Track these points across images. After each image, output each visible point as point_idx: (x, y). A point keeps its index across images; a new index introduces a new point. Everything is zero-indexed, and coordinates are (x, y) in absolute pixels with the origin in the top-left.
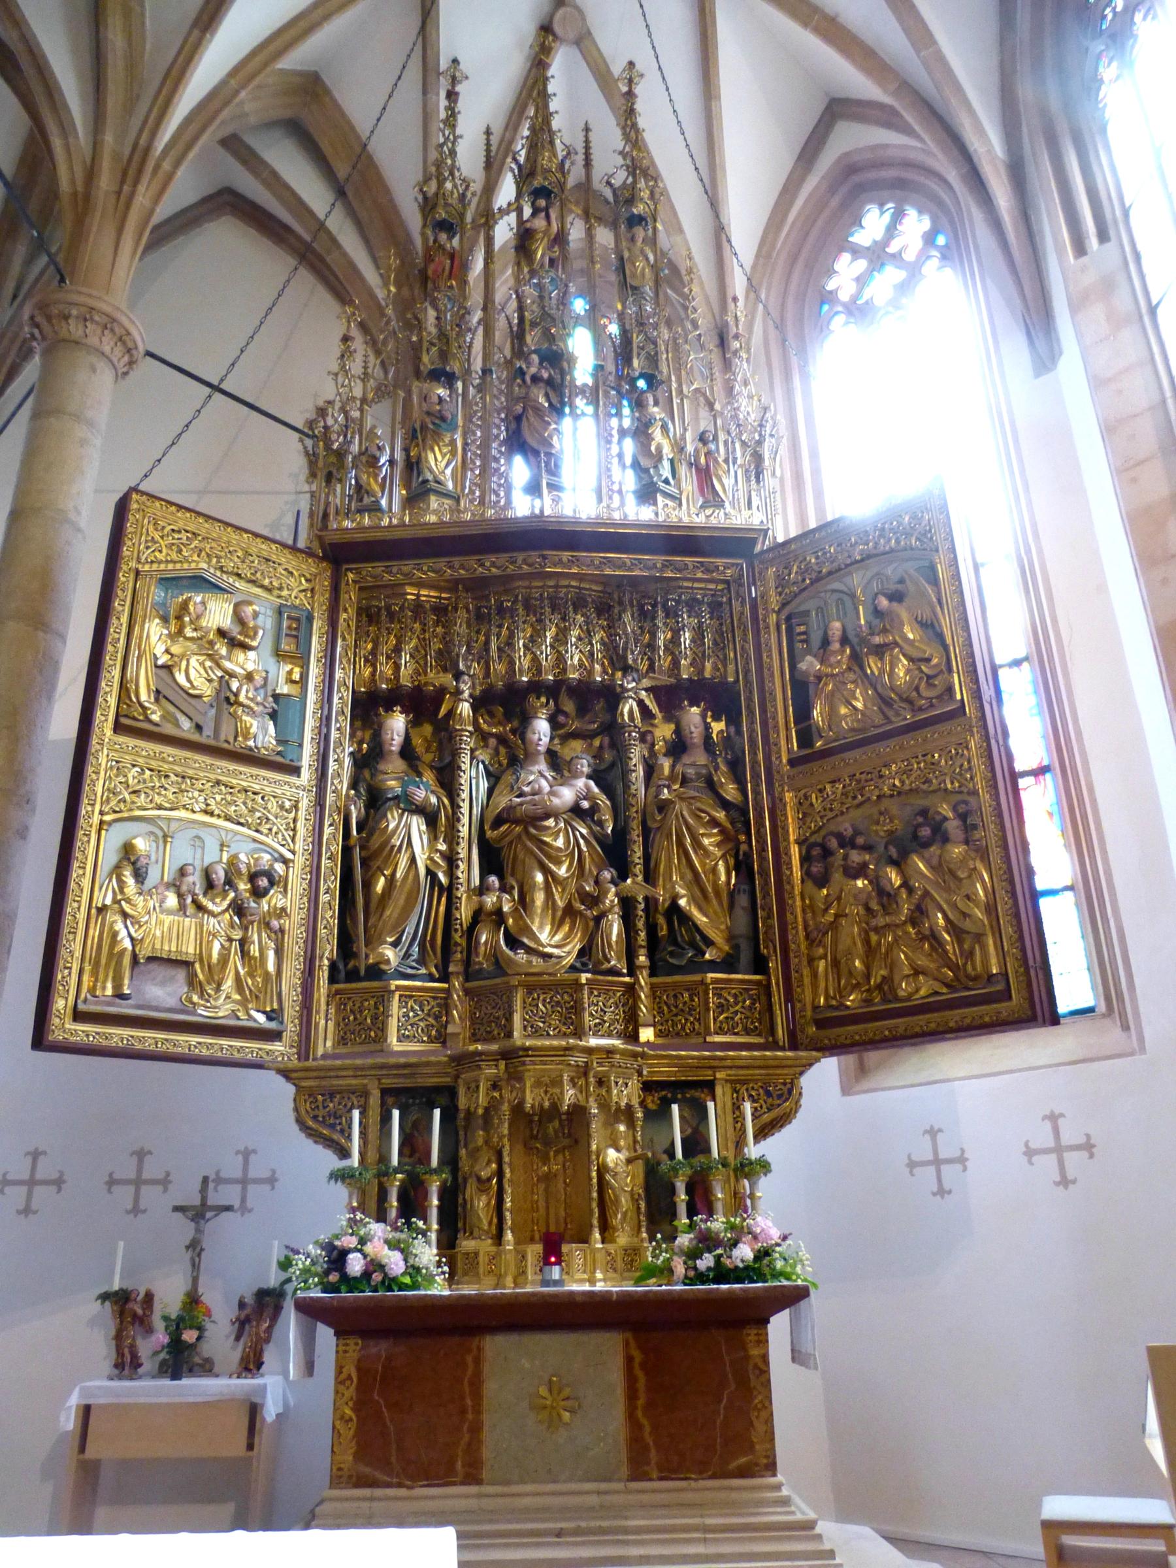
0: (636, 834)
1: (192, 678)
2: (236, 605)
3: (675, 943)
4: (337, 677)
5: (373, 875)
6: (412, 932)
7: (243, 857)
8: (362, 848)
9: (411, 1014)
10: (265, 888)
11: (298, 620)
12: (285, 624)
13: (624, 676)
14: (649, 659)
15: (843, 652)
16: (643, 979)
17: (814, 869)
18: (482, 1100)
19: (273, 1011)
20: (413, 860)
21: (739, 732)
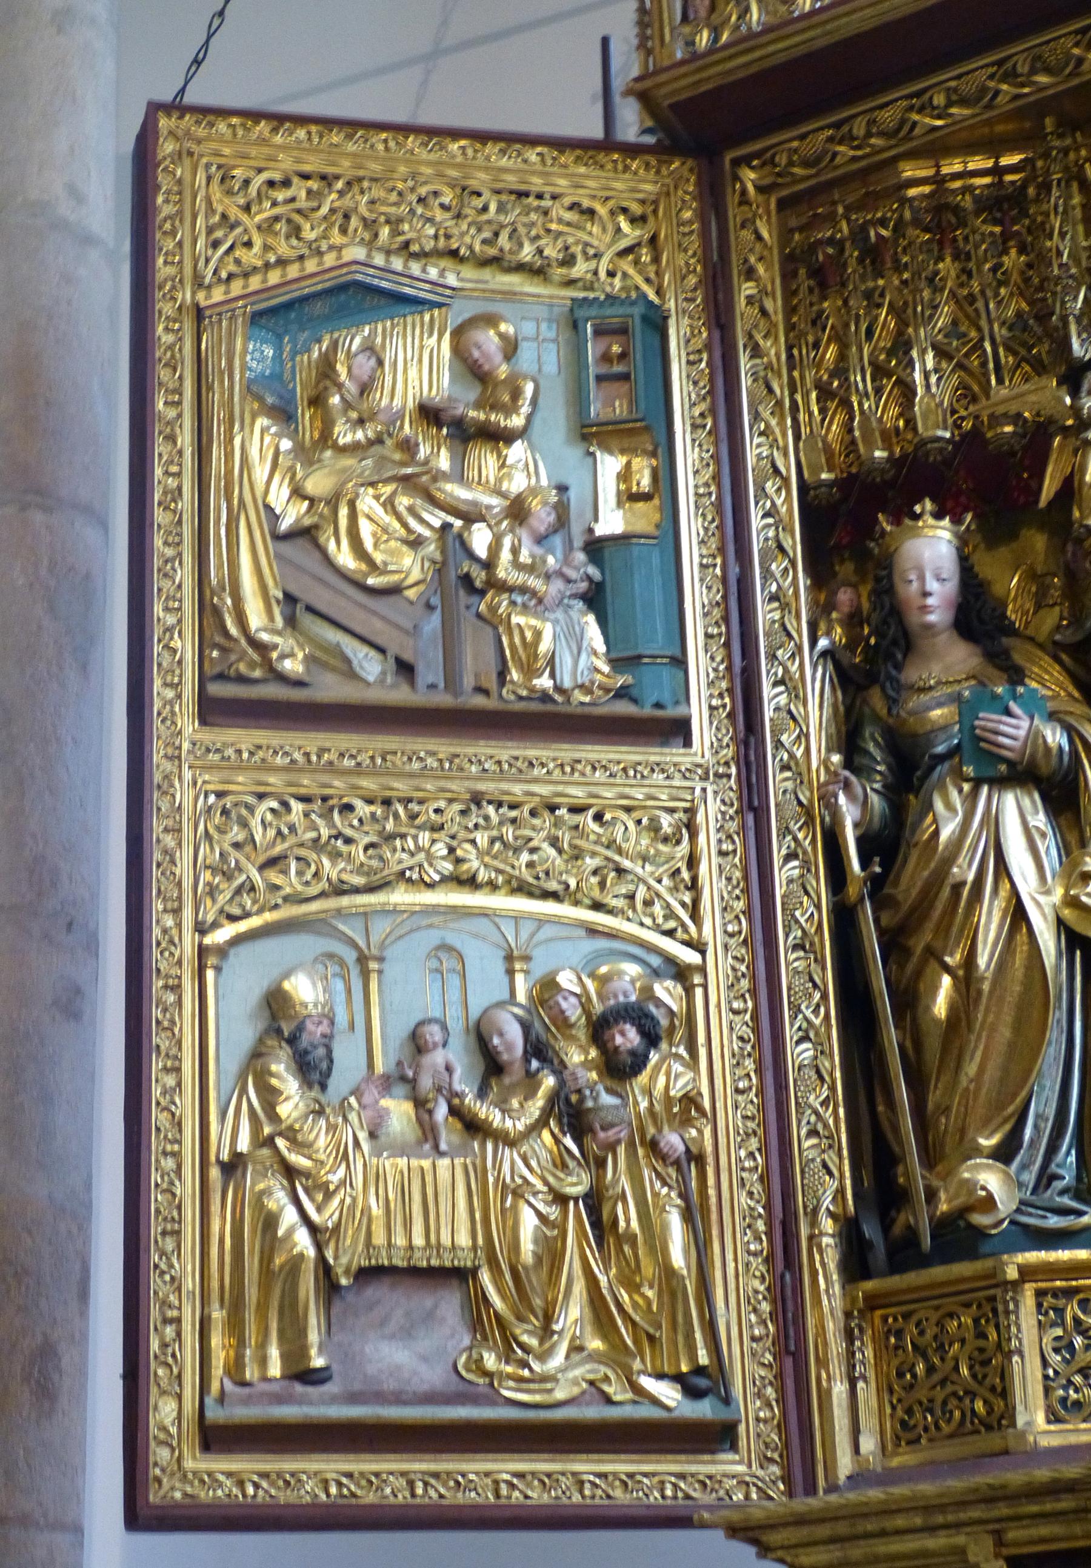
1: (368, 544)
2: (458, 333)
4: (750, 460)
6: (1051, 1112)
7: (566, 980)
10: (633, 1053)
11: (623, 331)
12: (592, 351)
19: (699, 1371)
20: (1018, 914)
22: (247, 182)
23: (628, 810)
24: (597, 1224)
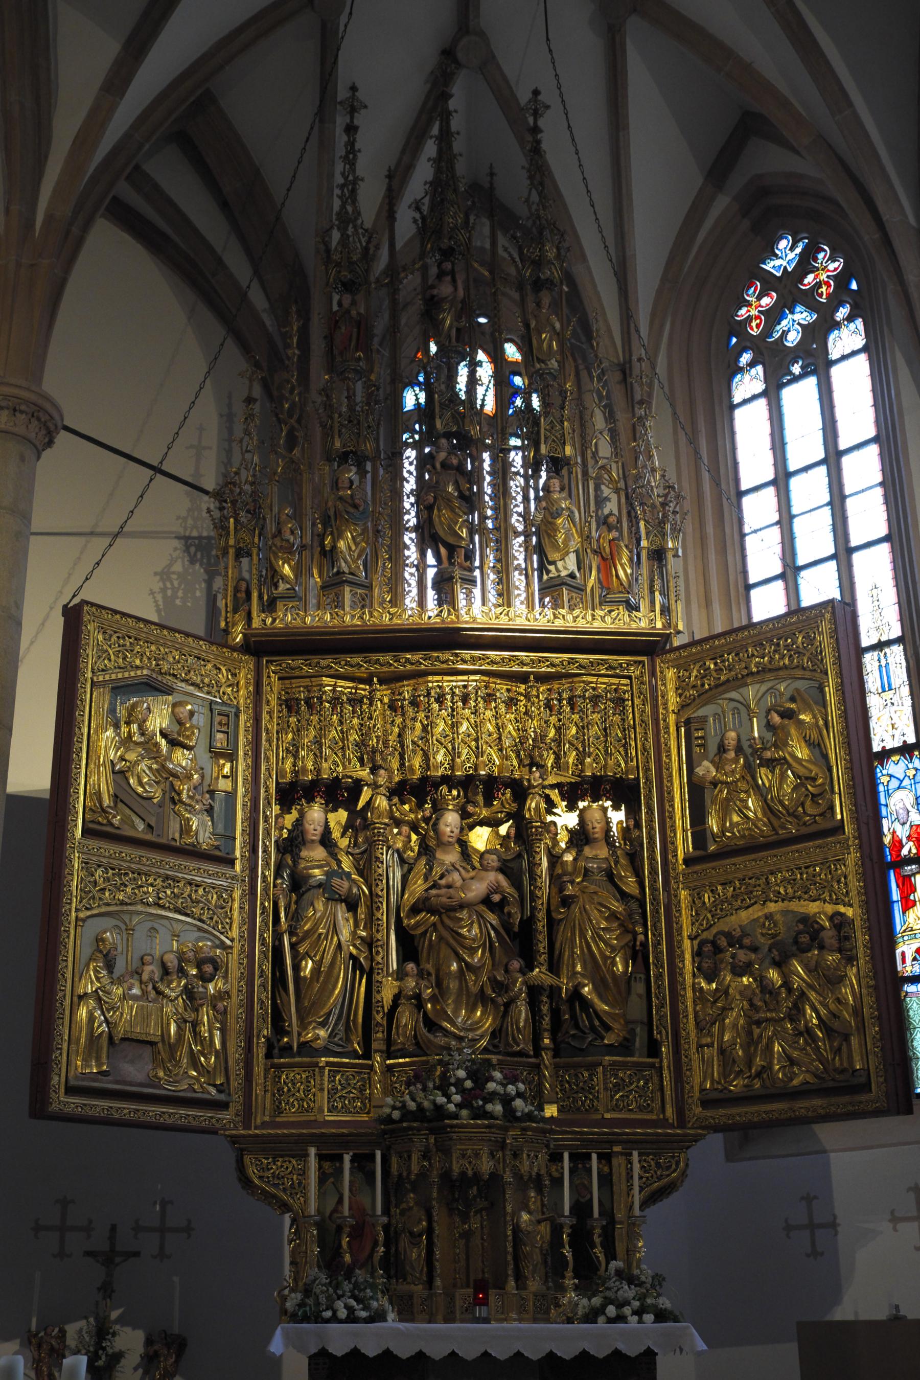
0: (541, 925)
2: (174, 705)
3: (577, 1026)
5: (301, 961)
6: (337, 1012)
8: (292, 934)
9: (339, 1087)
12: (217, 719)
14: (554, 753)
15: (736, 761)
16: (547, 1057)
17: (705, 965)
18: (415, 1168)
19: (222, 1084)
21: (638, 825)
22: (111, 636)
23: (214, 888)
24: (194, 1031)
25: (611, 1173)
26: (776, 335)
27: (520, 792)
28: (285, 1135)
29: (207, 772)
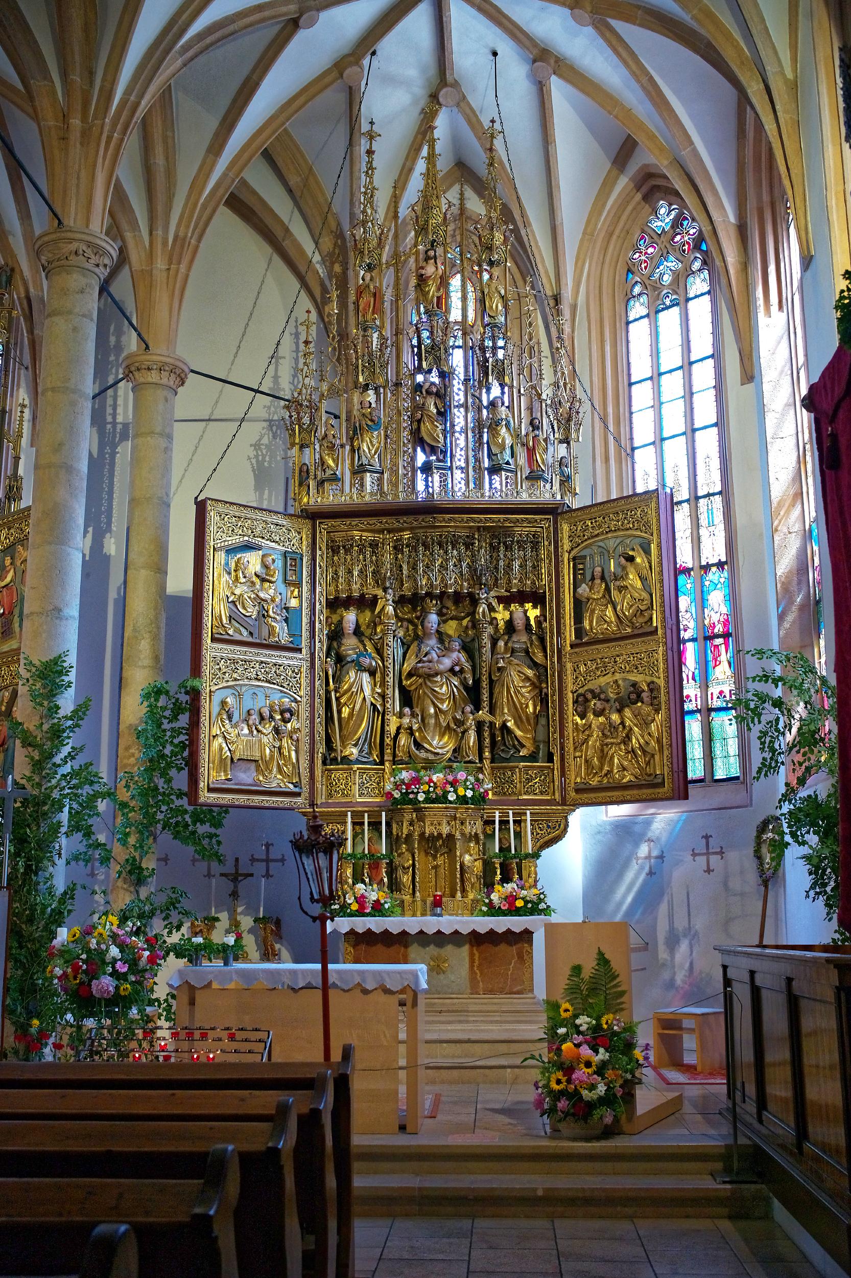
0: (485, 684)
8: (336, 692)
13: (481, 589)
16: (487, 763)
17: (579, 709)
18: (405, 832)
25: (521, 832)
26: (657, 276)
27: (474, 601)
28: (332, 812)
29: (284, 595)
